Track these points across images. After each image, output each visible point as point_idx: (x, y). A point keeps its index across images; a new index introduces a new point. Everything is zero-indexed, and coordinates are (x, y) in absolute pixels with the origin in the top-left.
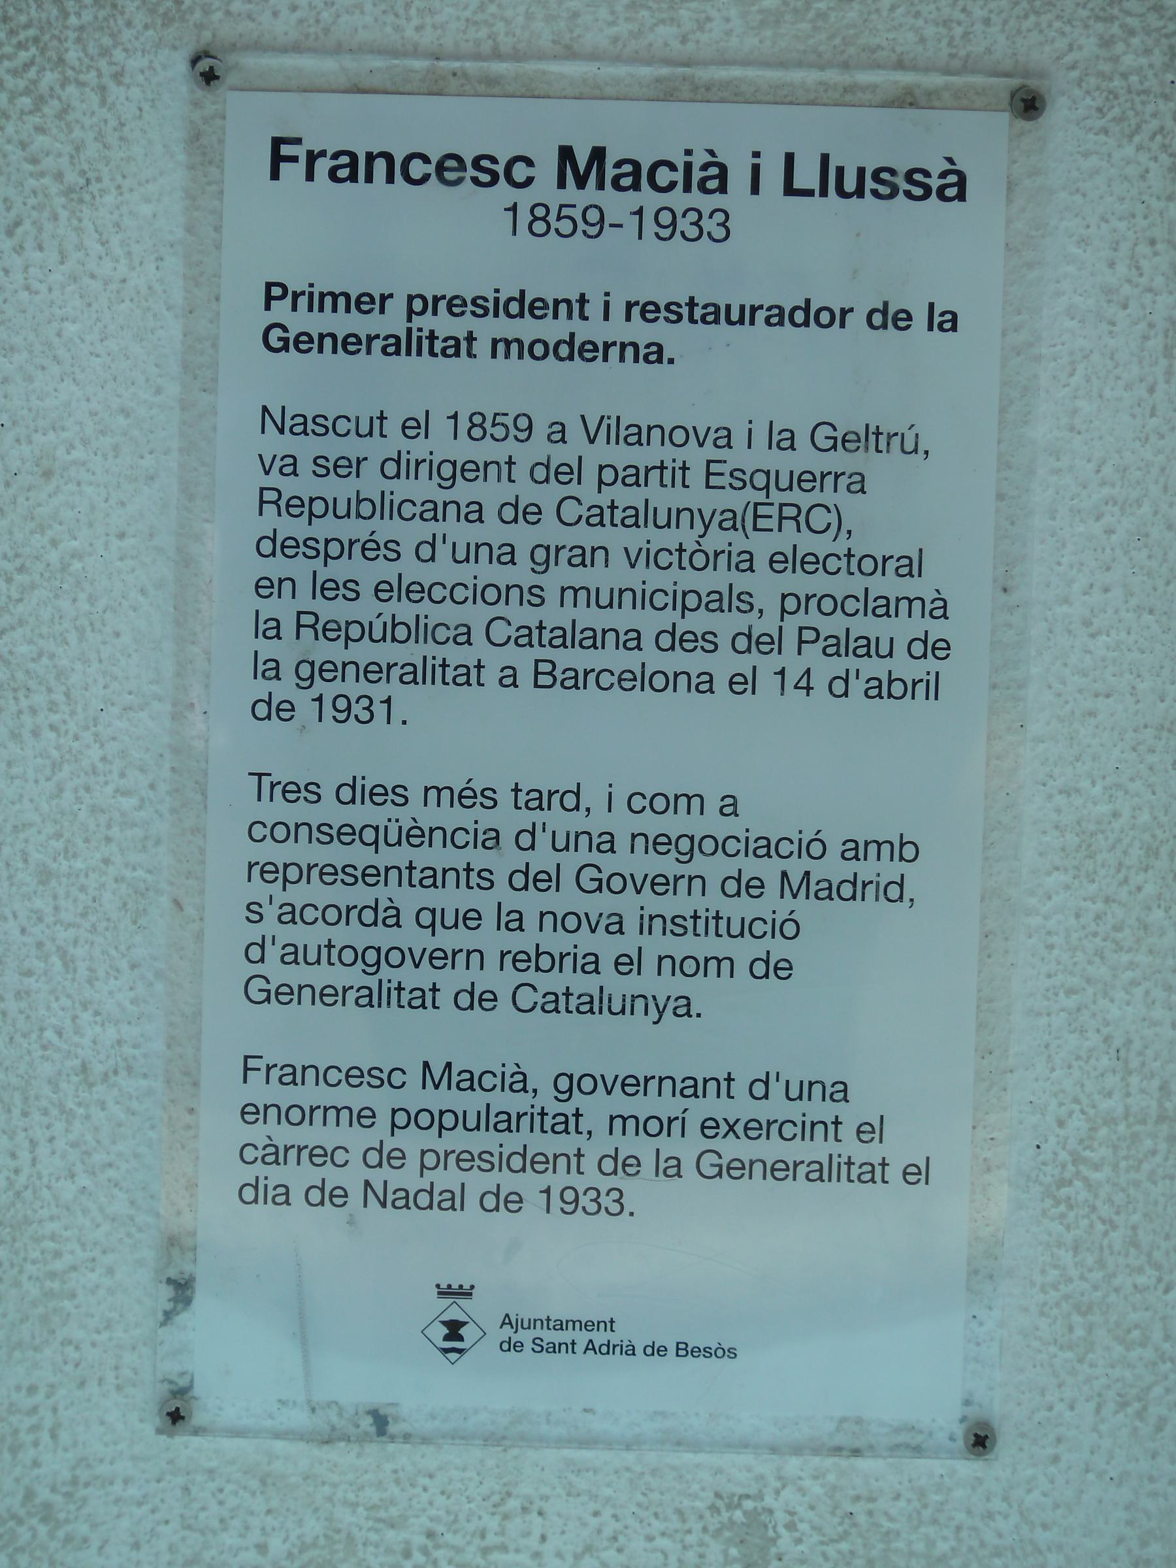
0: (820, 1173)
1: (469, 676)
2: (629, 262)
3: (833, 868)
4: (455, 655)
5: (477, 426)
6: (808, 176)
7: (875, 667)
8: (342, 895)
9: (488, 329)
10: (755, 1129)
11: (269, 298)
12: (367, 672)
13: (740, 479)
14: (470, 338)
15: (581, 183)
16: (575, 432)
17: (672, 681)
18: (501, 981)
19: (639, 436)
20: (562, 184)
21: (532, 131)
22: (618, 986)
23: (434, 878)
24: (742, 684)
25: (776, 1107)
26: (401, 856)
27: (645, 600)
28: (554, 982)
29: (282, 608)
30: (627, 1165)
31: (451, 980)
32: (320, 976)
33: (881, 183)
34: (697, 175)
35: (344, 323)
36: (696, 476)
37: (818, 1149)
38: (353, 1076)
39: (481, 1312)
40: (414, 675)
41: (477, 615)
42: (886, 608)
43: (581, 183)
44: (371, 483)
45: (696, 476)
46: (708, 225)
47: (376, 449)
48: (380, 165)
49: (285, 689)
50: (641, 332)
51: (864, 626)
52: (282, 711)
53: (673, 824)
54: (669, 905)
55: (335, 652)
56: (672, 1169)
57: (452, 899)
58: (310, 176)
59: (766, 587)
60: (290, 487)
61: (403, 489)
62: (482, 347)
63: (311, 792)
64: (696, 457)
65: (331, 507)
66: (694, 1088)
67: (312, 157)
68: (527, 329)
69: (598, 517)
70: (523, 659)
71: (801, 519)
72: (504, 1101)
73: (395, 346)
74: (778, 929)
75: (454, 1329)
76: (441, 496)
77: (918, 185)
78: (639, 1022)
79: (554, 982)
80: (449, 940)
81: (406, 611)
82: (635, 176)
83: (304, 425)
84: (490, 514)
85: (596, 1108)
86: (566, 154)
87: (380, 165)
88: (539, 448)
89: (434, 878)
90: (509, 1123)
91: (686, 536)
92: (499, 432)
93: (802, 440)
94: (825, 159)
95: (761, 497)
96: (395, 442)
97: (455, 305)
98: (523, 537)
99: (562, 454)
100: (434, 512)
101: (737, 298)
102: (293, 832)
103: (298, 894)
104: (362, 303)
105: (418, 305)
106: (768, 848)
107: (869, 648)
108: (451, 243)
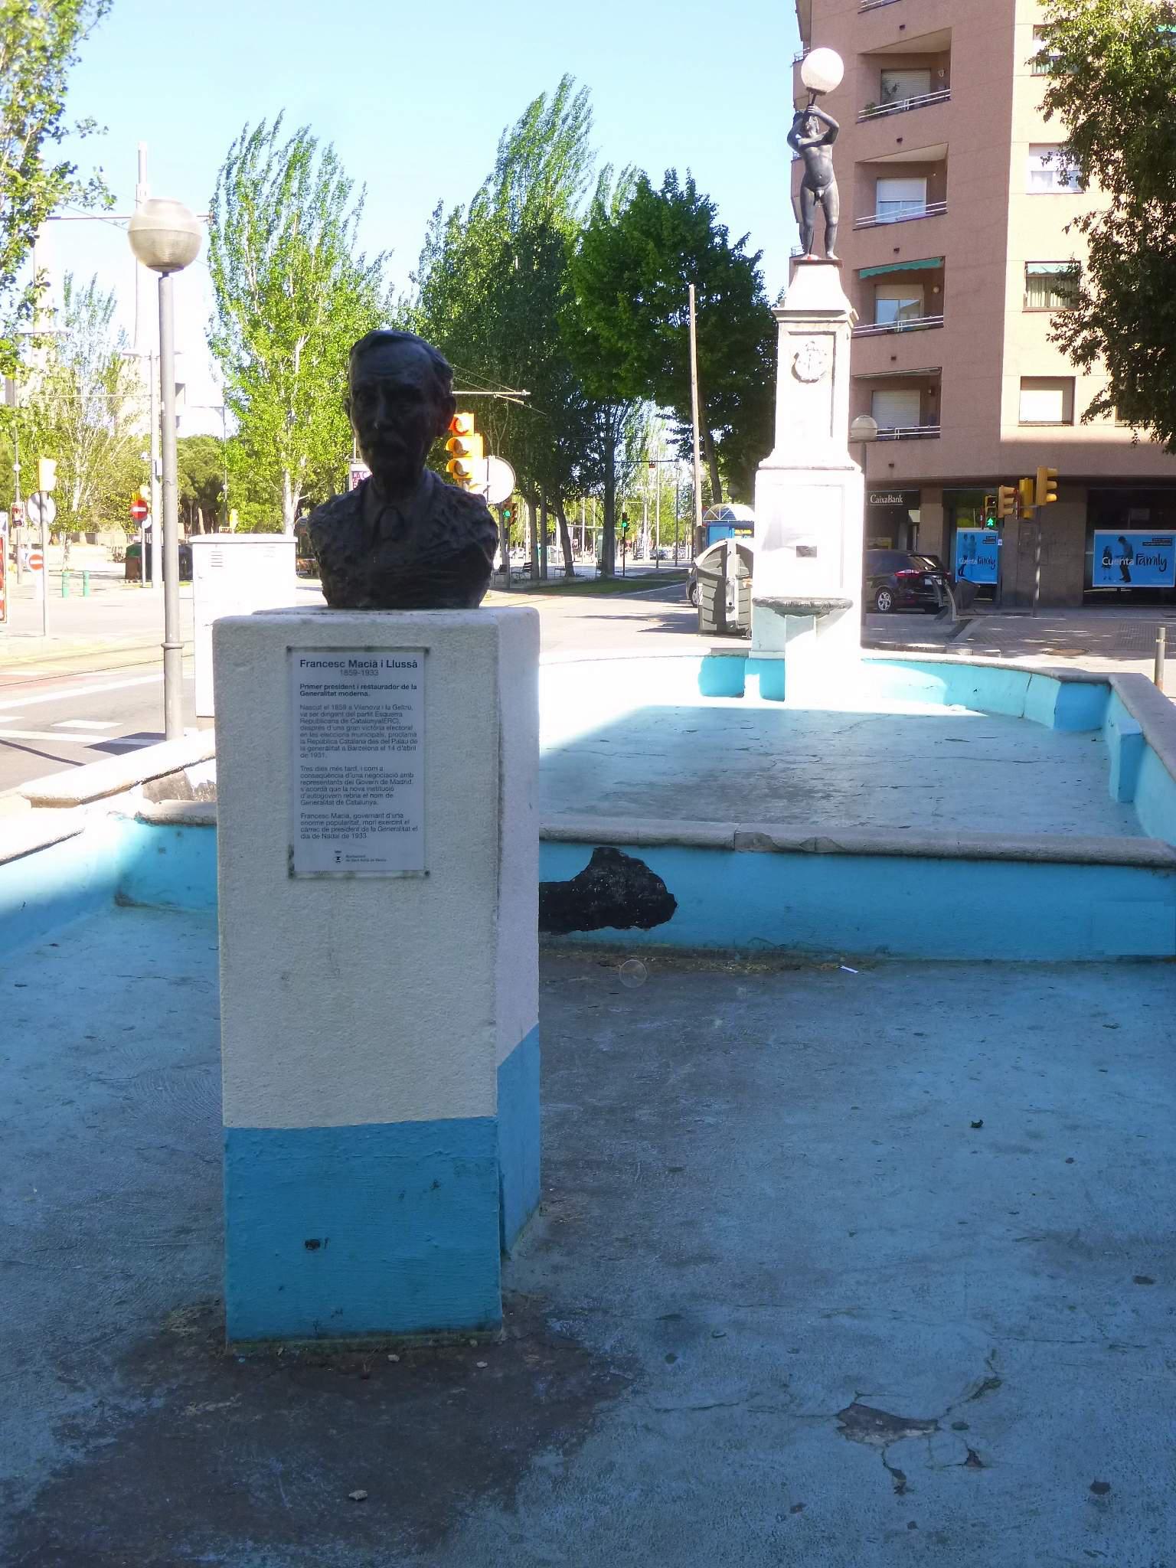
1: (337, 749)
5: (337, 707)
22: (364, 800)
24: (383, 749)
29: (305, 739)
39: (343, 855)
52: (305, 756)
56: (373, 830)
57: (335, 786)
59: (386, 732)
66: (377, 816)
82: (361, 665)
83: (308, 708)
85: (361, 820)
108: (332, 677)
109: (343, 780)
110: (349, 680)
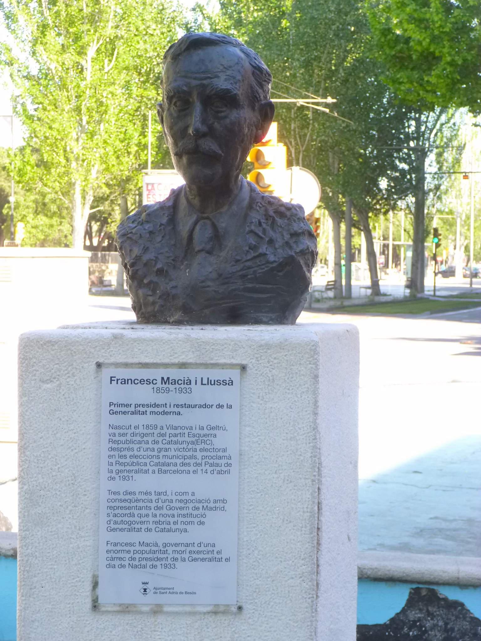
0: (210, 560)
1: (147, 472)
2: (175, 397)
3: (212, 505)
4: (144, 468)
5: (148, 426)
6: (205, 381)
7: (219, 469)
8: (124, 512)
9: (149, 410)
10: (198, 552)
11: (110, 405)
12: (128, 471)
13: (194, 436)
14: (146, 411)
15: (165, 383)
16: (165, 428)
17: (182, 472)
18: (153, 526)
19: (176, 428)
20: (162, 384)
21: (157, 374)
23: (141, 508)
24: (195, 472)
25: (202, 548)
26: (135, 504)
27: (178, 457)
28: (162, 526)
29: (113, 460)
30: (176, 559)
31: (144, 527)
32: (120, 526)
33: (218, 383)
34: (186, 382)
35: (124, 409)
36: (186, 435)
37: (210, 556)
38: (126, 544)
39: (150, 587)
40: (137, 472)
41: (148, 461)
42: (220, 458)
43: (165, 383)
44: (129, 438)
45: (186, 435)
46: (188, 390)
47: (130, 432)
48: (130, 381)
49: (113, 475)
50: (176, 410)
51: (216, 461)
52: (113, 479)
53: (183, 498)
54: (183, 512)
55: (122, 468)
56: (184, 560)
57: (144, 512)
58: (117, 383)
59: (199, 454)
60: (114, 439)
61: (134, 438)
62: (148, 413)
63: (118, 493)
64: (186, 431)
65: (122, 442)
66: (188, 545)
67: (117, 380)
68: (156, 410)
69: (169, 443)
70: (156, 468)
71: (205, 442)
72: (154, 548)
73: (133, 413)
74: (202, 516)
75: (145, 590)
76: (141, 440)
77: (224, 383)
78: (177, 533)
79: (162, 526)
80: (143, 519)
81: (135, 460)
82: (175, 382)
83: (117, 428)
84: (150, 442)
85: (170, 549)
86: (163, 378)
87: (130, 381)
88: (158, 431)
89: (141, 508)
90: (155, 552)
91: (185, 446)
92: (151, 428)
93: (205, 428)
94: (208, 378)
95: (198, 438)
96: (133, 430)
97: (143, 406)
98: (156, 447)
99: (162, 432)
100: (140, 442)
101: (193, 403)
102: (115, 501)
103: (116, 512)
104: (127, 406)
105: (137, 406)
106: (200, 501)
107: (217, 465)
109: (153, 505)
110: (160, 399)
